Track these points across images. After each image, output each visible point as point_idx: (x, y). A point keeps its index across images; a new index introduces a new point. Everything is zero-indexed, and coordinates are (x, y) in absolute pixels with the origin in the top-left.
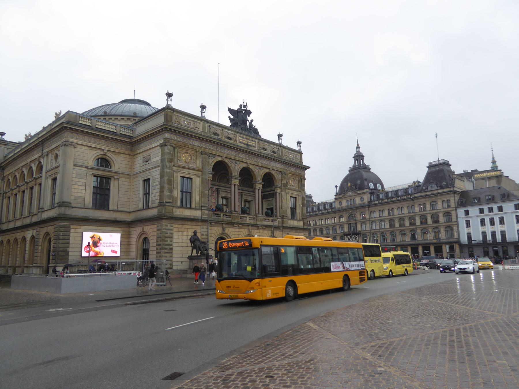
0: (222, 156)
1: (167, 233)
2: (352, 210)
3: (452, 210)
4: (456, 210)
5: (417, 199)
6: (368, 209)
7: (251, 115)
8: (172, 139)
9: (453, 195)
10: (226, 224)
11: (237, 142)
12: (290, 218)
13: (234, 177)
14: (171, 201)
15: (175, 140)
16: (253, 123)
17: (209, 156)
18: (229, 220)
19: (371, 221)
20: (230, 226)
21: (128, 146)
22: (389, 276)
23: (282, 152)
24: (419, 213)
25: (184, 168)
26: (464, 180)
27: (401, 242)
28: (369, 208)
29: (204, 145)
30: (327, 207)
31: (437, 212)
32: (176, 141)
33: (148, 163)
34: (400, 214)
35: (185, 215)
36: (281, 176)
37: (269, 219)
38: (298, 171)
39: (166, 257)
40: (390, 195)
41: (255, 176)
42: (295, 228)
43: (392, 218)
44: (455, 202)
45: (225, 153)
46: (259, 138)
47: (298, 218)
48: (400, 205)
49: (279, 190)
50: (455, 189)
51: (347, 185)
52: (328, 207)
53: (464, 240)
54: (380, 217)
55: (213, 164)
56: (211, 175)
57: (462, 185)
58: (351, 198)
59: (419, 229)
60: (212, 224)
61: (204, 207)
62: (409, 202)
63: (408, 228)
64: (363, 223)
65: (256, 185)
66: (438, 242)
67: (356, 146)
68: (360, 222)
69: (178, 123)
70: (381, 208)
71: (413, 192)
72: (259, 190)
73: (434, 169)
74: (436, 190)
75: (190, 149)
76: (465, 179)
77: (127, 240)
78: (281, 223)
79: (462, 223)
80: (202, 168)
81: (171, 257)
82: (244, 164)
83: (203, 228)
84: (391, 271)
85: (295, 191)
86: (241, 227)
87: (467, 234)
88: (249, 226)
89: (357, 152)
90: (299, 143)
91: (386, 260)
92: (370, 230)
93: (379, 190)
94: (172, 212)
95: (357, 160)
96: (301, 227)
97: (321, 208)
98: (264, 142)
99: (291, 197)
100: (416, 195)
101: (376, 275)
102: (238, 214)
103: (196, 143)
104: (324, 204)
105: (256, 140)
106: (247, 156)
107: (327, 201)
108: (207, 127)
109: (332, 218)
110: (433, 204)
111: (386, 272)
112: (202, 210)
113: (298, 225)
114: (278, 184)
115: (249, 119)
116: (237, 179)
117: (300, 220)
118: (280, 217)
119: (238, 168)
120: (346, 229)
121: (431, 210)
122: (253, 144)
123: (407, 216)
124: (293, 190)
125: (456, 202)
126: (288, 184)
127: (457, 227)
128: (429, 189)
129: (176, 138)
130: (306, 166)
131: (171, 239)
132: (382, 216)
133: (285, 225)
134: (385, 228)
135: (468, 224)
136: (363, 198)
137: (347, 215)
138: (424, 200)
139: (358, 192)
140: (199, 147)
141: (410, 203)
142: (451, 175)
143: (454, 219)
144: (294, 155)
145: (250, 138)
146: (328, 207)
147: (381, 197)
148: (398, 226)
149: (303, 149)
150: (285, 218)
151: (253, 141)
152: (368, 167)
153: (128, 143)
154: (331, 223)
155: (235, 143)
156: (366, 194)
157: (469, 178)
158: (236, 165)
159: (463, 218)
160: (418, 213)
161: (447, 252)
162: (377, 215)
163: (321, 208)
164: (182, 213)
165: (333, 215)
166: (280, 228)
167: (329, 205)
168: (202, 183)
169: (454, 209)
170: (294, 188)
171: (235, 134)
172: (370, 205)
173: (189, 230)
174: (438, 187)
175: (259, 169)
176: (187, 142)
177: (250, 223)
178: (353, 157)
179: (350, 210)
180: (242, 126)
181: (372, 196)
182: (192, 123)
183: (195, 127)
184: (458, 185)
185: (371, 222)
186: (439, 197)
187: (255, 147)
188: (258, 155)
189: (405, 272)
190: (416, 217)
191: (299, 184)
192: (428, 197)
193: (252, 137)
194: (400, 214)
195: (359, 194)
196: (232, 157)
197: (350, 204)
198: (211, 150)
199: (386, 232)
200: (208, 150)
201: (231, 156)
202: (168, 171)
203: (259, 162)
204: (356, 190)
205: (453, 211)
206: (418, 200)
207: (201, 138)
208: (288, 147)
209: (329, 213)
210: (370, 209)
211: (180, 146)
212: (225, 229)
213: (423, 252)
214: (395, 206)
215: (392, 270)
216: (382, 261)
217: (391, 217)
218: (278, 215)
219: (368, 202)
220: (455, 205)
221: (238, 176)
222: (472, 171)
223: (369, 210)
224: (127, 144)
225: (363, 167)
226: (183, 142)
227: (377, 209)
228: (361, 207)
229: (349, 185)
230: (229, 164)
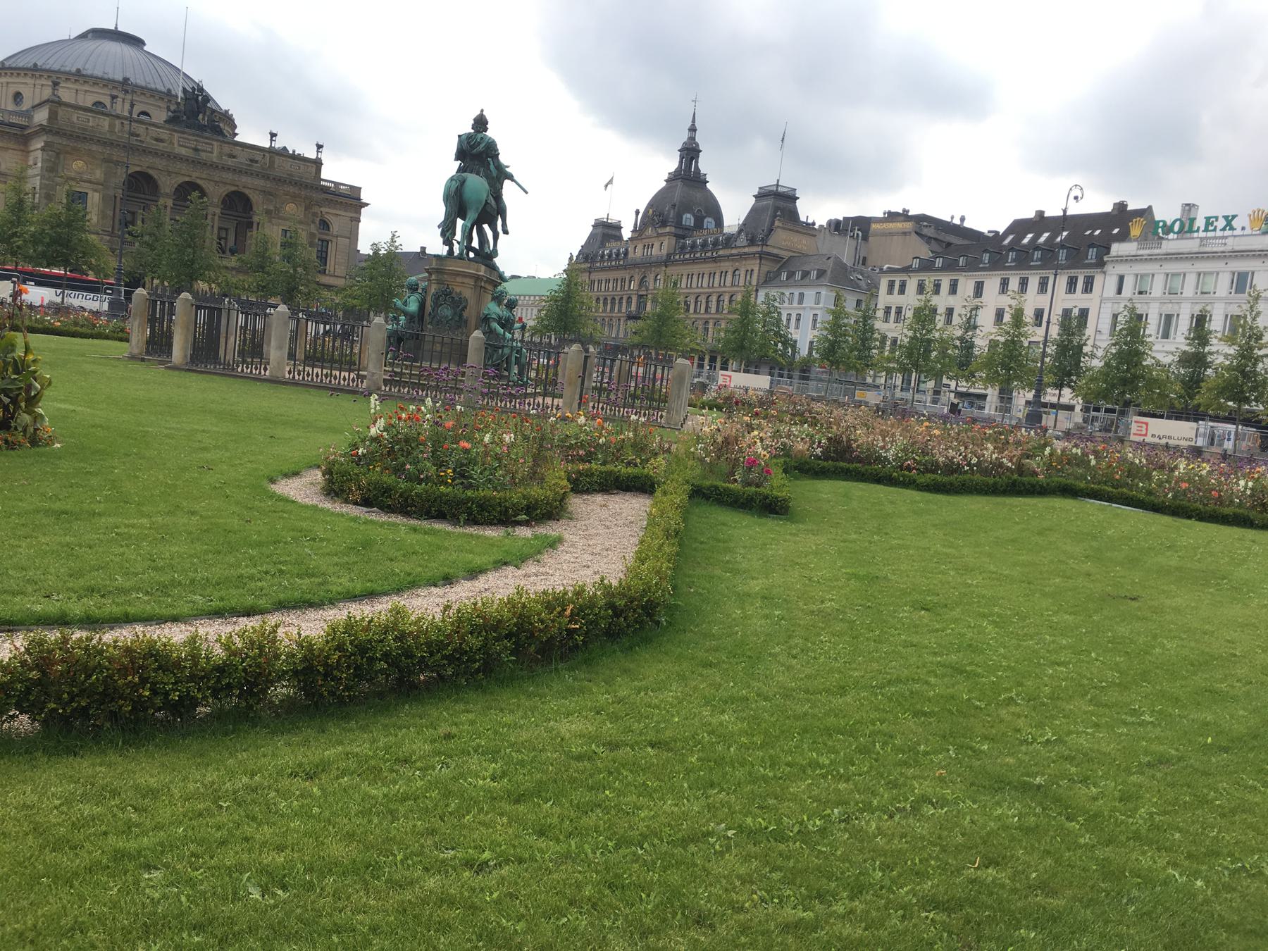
4: (757, 290)
5: (720, 261)
6: (664, 268)
49: (256, 219)
50: (765, 249)
89: (689, 138)
120: (633, 307)
138: (727, 264)
149: (325, 157)
172: (668, 261)
192: (733, 260)
195: (659, 235)
220: (758, 282)
229: (651, 211)
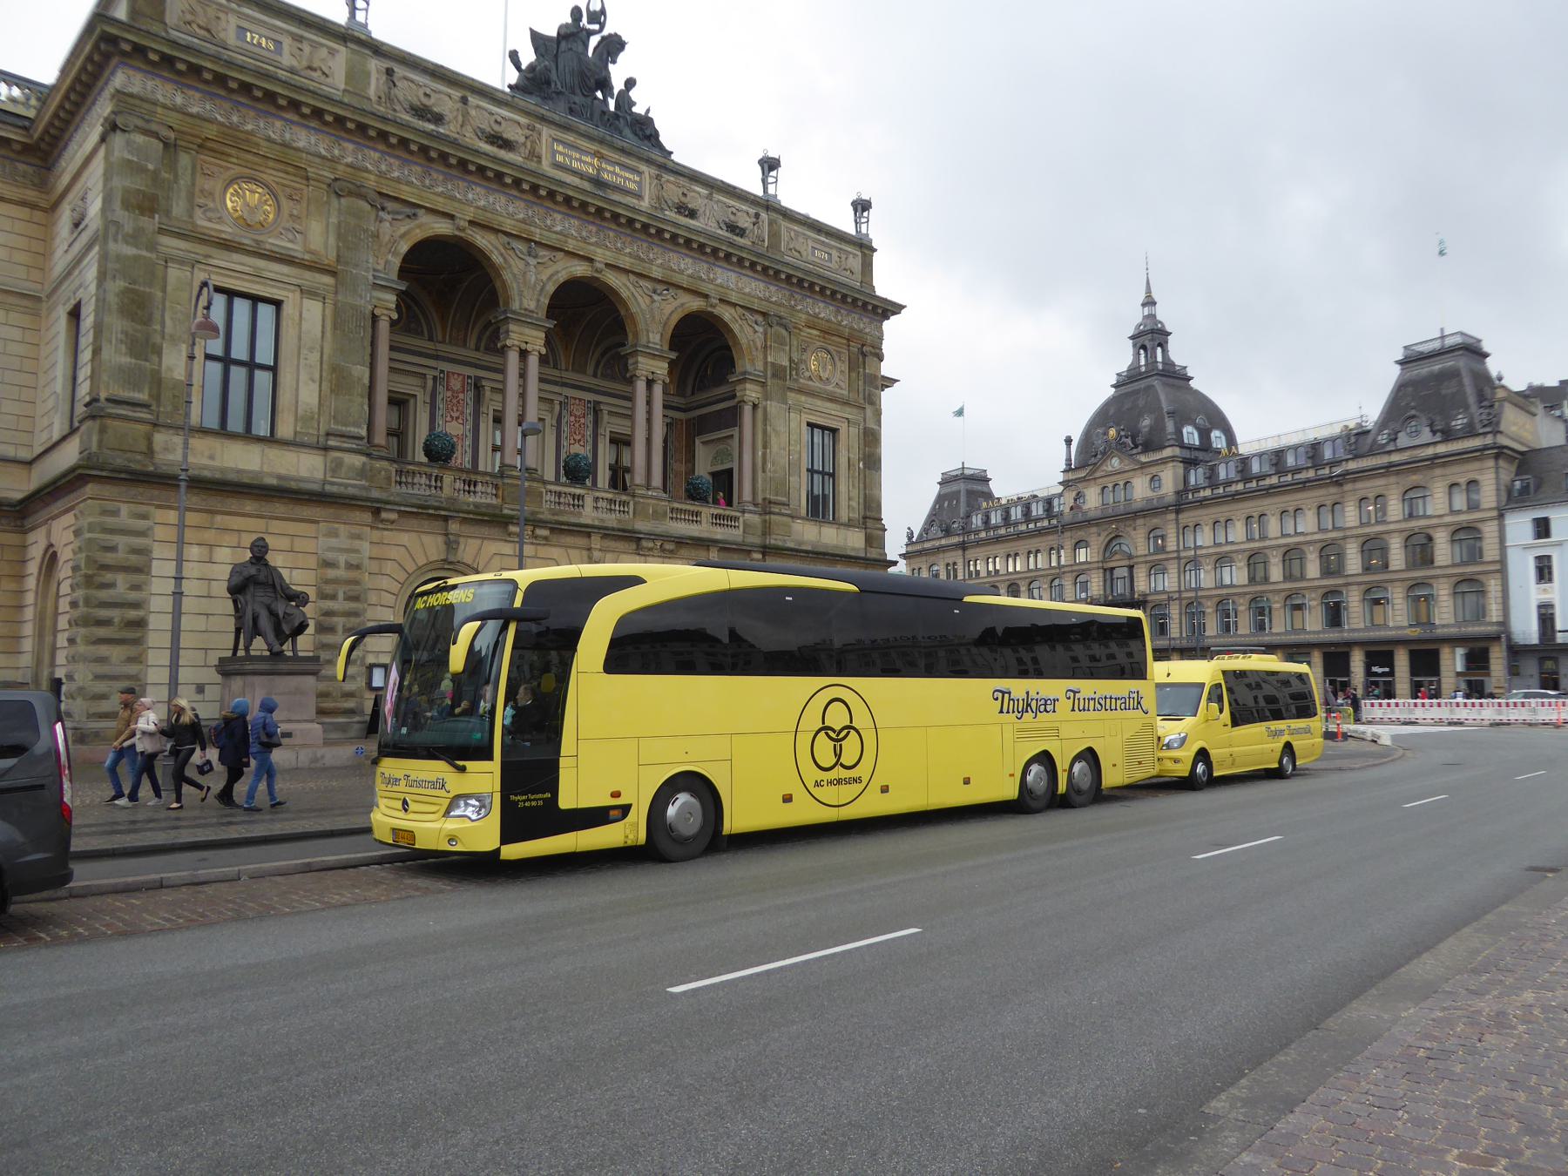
0: (452, 217)
1: (113, 549)
2: (1119, 519)
3: (1483, 520)
4: (1501, 516)
5: (1354, 480)
6: (1173, 516)
7: (621, 57)
8: (155, 103)
9: (1491, 463)
10: (464, 521)
11: (539, 162)
12: (803, 512)
13: (514, 312)
14: (143, 396)
15: (175, 109)
16: (633, 94)
17: (383, 209)
18: (489, 505)
19: (1185, 557)
20: (485, 531)
21: (21, 167)
22: (1187, 784)
23: (775, 235)
24: (1361, 531)
25: (227, 246)
26: (1533, 409)
27: (1287, 633)
28: (1178, 512)
29: (349, 152)
30: (1034, 513)
31: (1429, 527)
32: (180, 116)
33: (81, 227)
34: (1289, 535)
35: (223, 470)
36: (765, 334)
37: (698, 514)
38: (850, 321)
39: (102, 660)
40: (1255, 468)
41: (635, 324)
42: (825, 554)
43: (1260, 548)
44: (1498, 490)
45: (469, 203)
46: (661, 160)
47: (844, 515)
48: (1290, 501)
49: (751, 392)
51: (1106, 433)
52: (1037, 510)
53: (1526, 629)
54: (1216, 545)
55: (404, 248)
56: (394, 298)
57: (1527, 426)
58: (1113, 478)
59: (1355, 587)
60: (384, 515)
61: (342, 436)
62: (1322, 492)
63: (1316, 583)
64: (1156, 567)
65: (637, 362)
66: (1427, 635)
67: (1142, 297)
68: (1146, 562)
69: (202, 33)
70: (1220, 512)
71: (1341, 454)
72: (650, 383)
73: (1424, 370)
74: (1428, 445)
75: (271, 164)
76: (1539, 409)
77: (13, 586)
78: (760, 533)
79: (1522, 567)
80: (338, 256)
81: (137, 659)
82: (576, 262)
83: (334, 534)
84: (1203, 755)
85: (831, 400)
86: (546, 538)
87: (1540, 607)
88: (589, 535)
89: (1145, 317)
90: (862, 206)
91: (1179, 700)
92: (1180, 592)
93: (1218, 452)
94: (144, 449)
95: (1144, 347)
96: (853, 554)
97: (1016, 514)
98: (682, 181)
99: (811, 425)
100: (1352, 465)
101: (1112, 777)
102: (534, 480)
103: (304, 138)
104: (1026, 504)
105: (643, 167)
106: (594, 229)
107: (1035, 493)
108: (374, 76)
109: (1052, 549)
110: (1413, 495)
111: (1176, 761)
112: (326, 449)
113: (841, 543)
114: (750, 361)
115: (618, 74)
116: (537, 327)
117: (849, 524)
118: (756, 505)
119: (544, 278)
121: (1405, 520)
122: (628, 180)
123: (1315, 542)
124: (823, 399)
125: (1503, 488)
126: (797, 369)
127: (1499, 582)
128: (1403, 440)
129: (179, 100)
130: (886, 300)
131: (137, 578)
132: (1224, 542)
133: (773, 541)
134: (1232, 586)
135: (1544, 571)
136: (1160, 480)
137: (1101, 538)
139: (1143, 459)
140: (323, 158)
141: (1327, 494)
142: (1487, 390)
143: (1490, 551)
144: (835, 254)
145: (616, 156)
146: (1037, 510)
147: (1222, 475)
148: (1281, 579)
149: (876, 230)
150: (776, 509)
151: (624, 167)
152: (1182, 372)
153: (17, 147)
154: (1047, 567)
155: (532, 165)
156: (1171, 464)
157: (1552, 408)
158: (532, 261)
159: (1527, 547)
160: (1355, 532)
161: (1459, 674)
162: (1204, 538)
163: (1016, 514)
164: (212, 457)
165: (1052, 540)
166: (749, 552)
167: (1041, 505)
168: (335, 327)
169: (1495, 513)
170: (830, 388)
171: (530, 128)
172: (1182, 503)
173: (300, 544)
174: (1434, 432)
175: (655, 292)
176: (249, 127)
177: (596, 523)
178: (1131, 338)
179: (1111, 522)
180: (578, 99)
181: (1192, 472)
182: (287, 42)
183: (305, 64)
184: (1514, 429)
185: (1183, 561)
186: (1438, 471)
187: (639, 197)
188: (646, 227)
189: (1280, 762)
190: (1348, 546)
191: (854, 375)
192: (1398, 473)
193: (623, 151)
194: (1289, 535)
195: (1144, 466)
196: (508, 225)
197: (1112, 501)
198: (392, 179)
199: (1236, 598)
200: (372, 177)
201: (501, 219)
202: (129, 251)
203: (651, 262)
204: (1135, 451)
205: (1490, 523)
206: (1359, 485)
207: (308, 105)
208: (809, 218)
209: (1040, 533)
210: (1180, 516)
211: (209, 144)
212: (458, 543)
213: (1369, 673)
214: (1271, 505)
215: (1212, 752)
216: (1149, 701)
217: (1257, 545)
218: (747, 496)
219: (1177, 493)
221: (542, 314)
222: (1562, 382)
223: (1177, 520)
224: (12, 155)
225: (1163, 370)
226: (222, 124)
227: (1206, 516)
228: (1152, 510)
229: (1112, 432)
230: (496, 258)
